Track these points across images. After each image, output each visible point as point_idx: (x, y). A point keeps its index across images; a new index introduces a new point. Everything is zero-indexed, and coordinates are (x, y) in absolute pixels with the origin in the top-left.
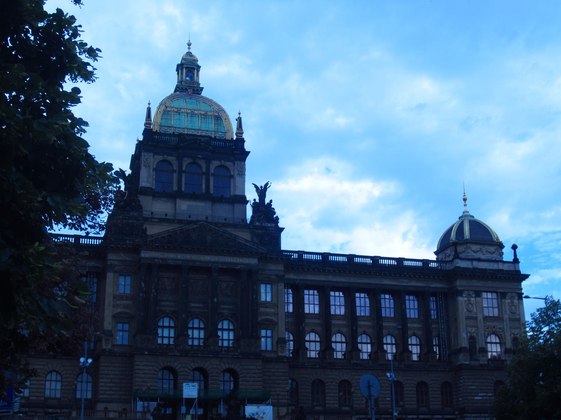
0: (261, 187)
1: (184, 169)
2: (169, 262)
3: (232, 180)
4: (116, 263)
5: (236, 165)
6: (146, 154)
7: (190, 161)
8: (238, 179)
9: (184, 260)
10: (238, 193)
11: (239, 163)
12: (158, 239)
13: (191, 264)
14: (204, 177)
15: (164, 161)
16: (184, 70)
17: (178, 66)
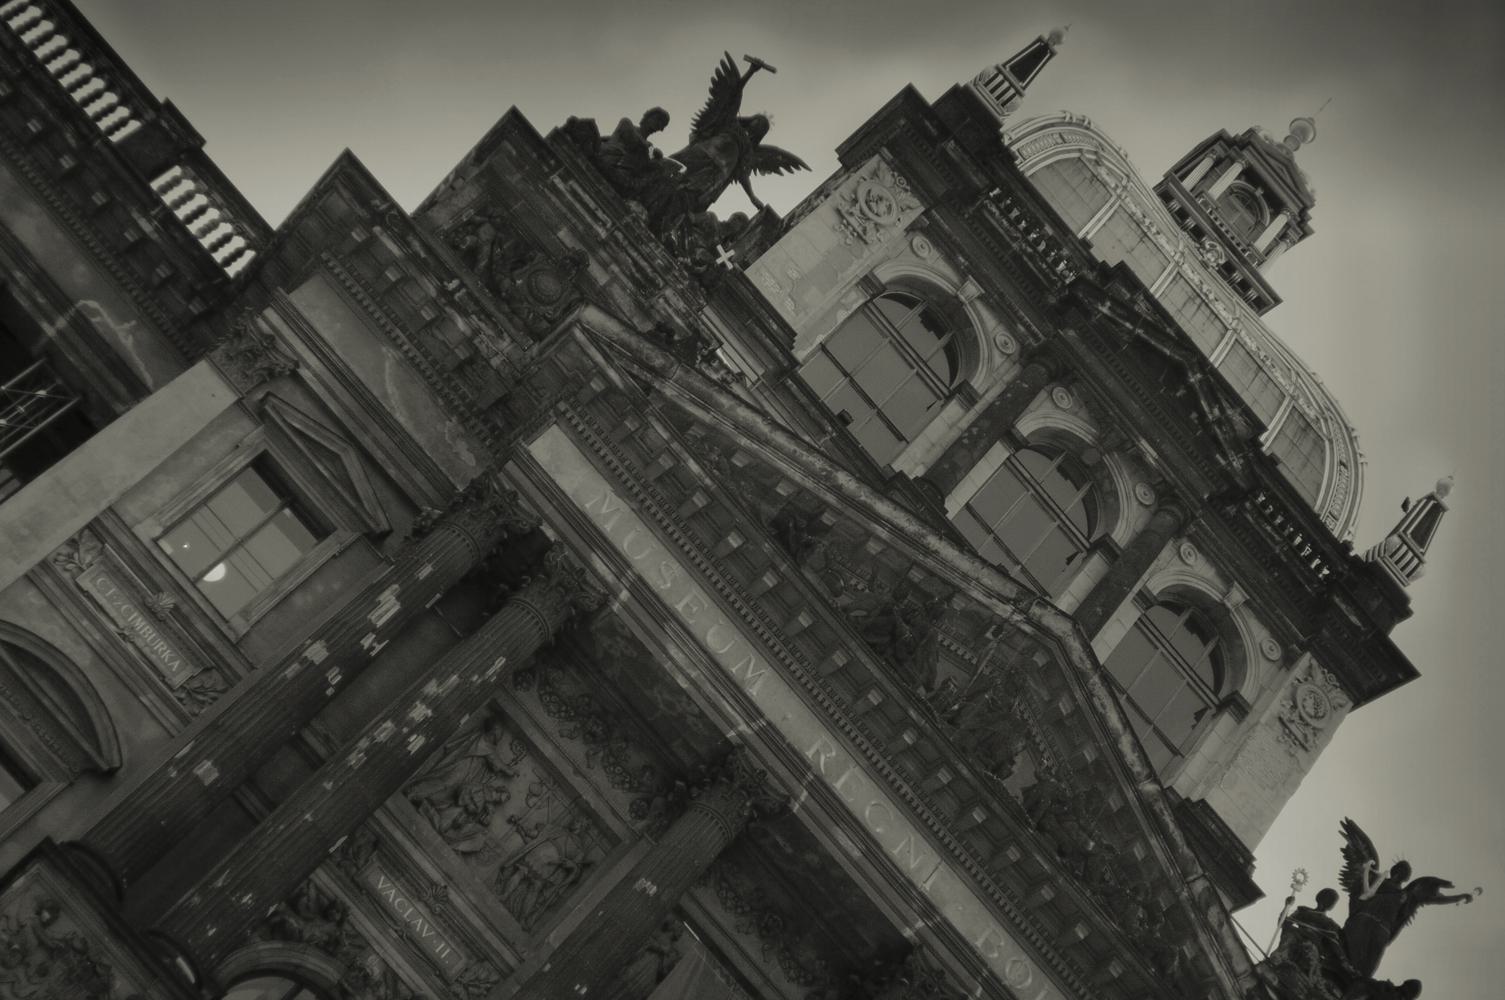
0: (1401, 869)
1: (1026, 426)
2: (673, 651)
3: (1226, 720)
4: (312, 367)
5: (1299, 670)
6: (888, 177)
7: (1080, 427)
8: (1263, 737)
9: (771, 734)
10: (1225, 804)
11: (1319, 677)
12: (730, 450)
13: (802, 800)
14: (1096, 565)
15: (941, 314)
16: (1236, 169)
17: (1220, 138)
